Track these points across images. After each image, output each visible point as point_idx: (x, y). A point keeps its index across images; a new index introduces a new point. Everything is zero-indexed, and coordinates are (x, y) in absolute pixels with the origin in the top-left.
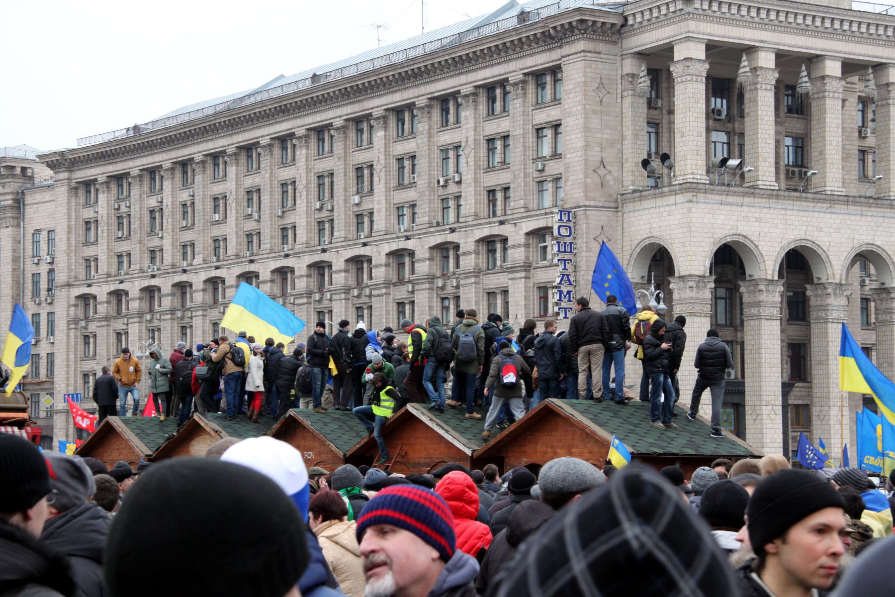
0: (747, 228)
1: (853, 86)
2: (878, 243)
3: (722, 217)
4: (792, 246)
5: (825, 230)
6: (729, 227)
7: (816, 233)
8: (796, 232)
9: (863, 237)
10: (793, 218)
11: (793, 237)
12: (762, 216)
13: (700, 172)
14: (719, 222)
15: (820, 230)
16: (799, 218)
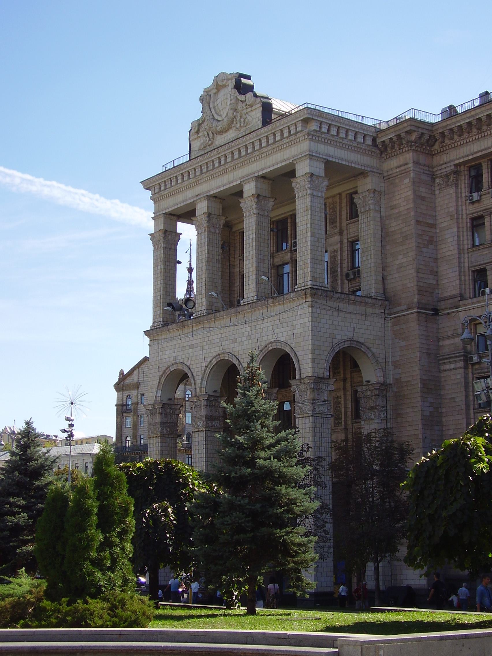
0: (183, 356)
1: (407, 166)
2: (282, 339)
3: (168, 352)
4: (214, 362)
5: (239, 340)
6: (172, 359)
7: (232, 345)
8: (217, 349)
9: (270, 337)
10: (215, 337)
11: (215, 354)
12: (194, 342)
13: (159, 320)
14: (166, 356)
15: (235, 341)
16: (219, 336)
